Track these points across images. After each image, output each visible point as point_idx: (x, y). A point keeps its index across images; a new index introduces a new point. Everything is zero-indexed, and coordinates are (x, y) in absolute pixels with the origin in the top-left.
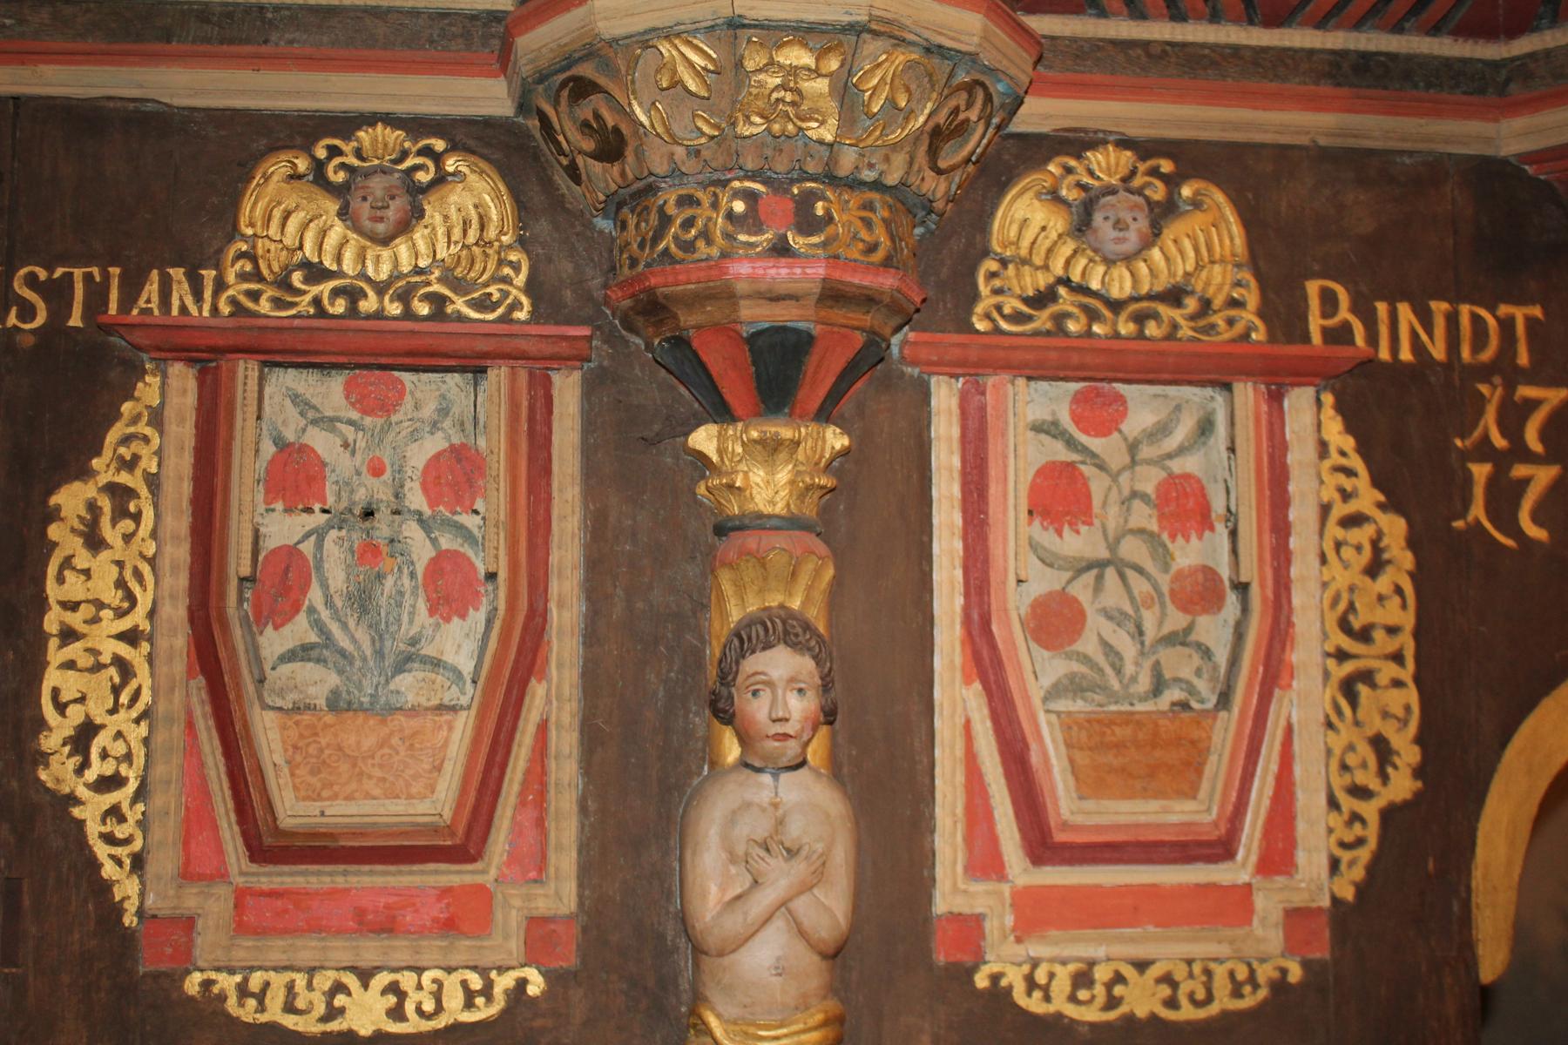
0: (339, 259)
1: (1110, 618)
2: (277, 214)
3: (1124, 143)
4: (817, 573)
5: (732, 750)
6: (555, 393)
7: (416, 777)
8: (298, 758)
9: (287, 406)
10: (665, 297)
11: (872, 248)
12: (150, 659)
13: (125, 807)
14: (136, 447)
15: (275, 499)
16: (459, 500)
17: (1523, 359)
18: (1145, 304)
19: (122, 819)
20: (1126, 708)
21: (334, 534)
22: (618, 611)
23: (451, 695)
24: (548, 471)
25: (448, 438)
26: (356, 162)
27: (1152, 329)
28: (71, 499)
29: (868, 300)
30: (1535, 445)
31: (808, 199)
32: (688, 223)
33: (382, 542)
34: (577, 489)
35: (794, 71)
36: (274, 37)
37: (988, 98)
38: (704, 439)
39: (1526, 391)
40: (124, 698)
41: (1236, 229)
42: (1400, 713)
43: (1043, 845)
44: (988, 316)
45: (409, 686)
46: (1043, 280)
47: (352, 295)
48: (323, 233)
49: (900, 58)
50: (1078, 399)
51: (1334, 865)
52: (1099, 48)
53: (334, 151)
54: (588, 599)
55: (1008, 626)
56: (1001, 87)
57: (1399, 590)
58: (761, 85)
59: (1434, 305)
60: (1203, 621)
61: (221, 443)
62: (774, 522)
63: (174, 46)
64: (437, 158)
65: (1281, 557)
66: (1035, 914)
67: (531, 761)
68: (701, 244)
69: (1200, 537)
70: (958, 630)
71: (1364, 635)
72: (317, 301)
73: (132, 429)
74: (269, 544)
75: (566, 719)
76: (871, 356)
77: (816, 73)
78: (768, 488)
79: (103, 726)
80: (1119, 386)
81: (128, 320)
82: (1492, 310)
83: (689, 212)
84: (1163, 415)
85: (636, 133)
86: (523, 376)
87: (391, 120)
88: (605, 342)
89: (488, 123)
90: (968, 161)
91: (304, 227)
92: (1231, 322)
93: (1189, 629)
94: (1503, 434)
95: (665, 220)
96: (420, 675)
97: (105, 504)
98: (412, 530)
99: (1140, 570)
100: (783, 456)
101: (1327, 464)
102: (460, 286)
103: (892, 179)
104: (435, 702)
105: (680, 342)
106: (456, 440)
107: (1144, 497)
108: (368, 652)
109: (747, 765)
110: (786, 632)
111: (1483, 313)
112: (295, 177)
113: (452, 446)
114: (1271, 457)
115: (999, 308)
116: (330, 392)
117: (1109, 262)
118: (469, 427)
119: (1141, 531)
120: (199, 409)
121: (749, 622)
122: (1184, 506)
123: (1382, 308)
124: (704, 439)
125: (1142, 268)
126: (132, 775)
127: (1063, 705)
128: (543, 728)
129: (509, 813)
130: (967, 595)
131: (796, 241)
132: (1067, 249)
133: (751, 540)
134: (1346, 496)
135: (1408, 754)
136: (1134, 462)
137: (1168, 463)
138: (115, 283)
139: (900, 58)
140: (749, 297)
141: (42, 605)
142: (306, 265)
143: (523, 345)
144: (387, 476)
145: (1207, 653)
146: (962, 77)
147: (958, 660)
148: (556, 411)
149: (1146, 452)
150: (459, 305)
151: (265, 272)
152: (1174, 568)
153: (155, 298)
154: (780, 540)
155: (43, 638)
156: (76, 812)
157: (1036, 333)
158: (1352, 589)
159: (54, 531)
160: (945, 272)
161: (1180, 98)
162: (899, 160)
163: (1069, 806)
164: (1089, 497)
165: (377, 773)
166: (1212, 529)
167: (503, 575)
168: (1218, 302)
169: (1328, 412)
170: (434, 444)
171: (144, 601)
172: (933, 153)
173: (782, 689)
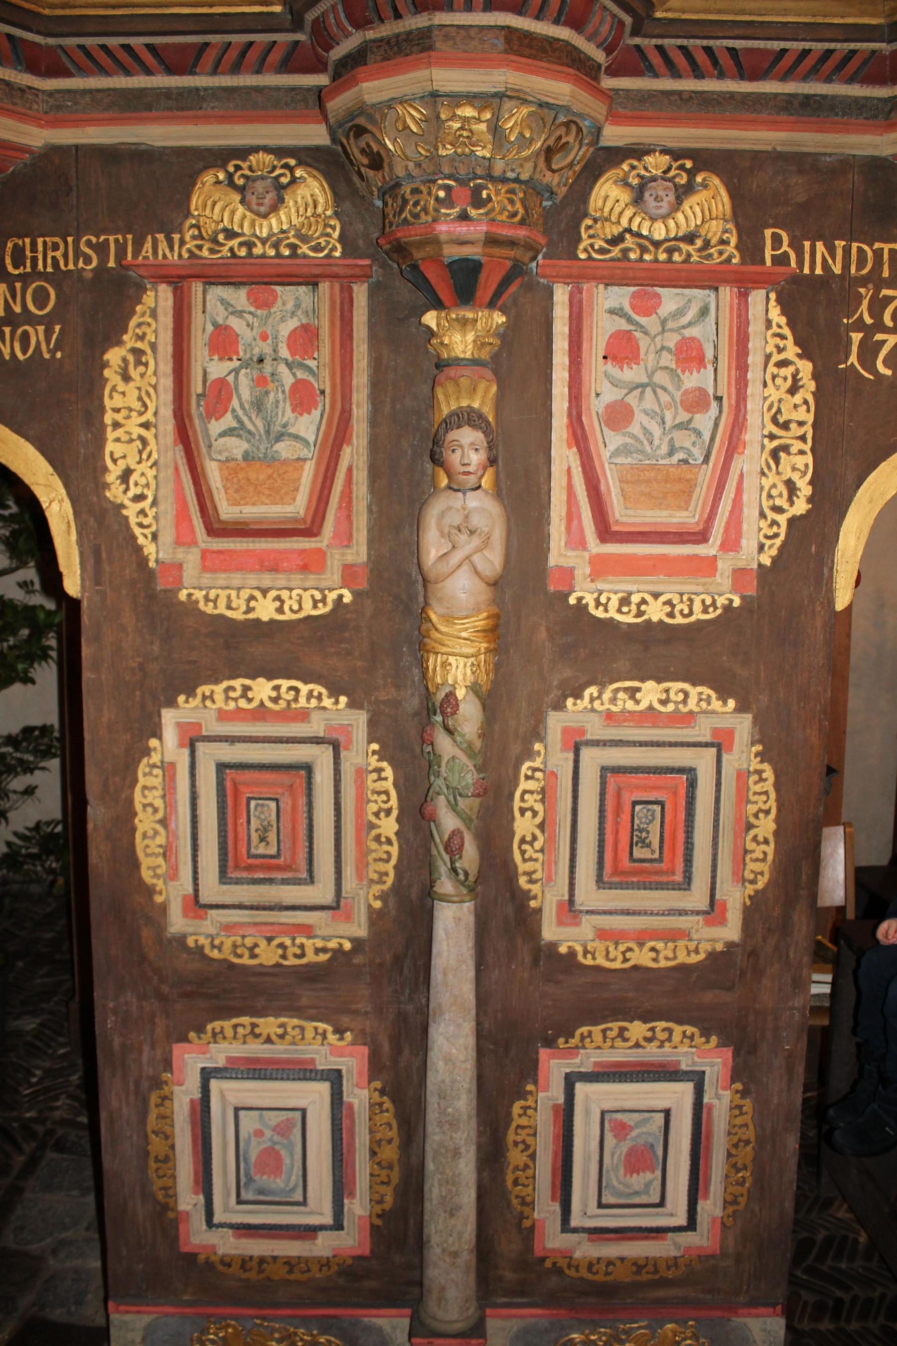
0: (242, 227)
1: (648, 415)
2: (209, 203)
3: (665, 152)
4: (487, 390)
5: (444, 482)
6: (354, 295)
7: (287, 493)
8: (228, 485)
10: (406, 243)
11: (514, 215)
12: (156, 436)
13: (147, 510)
14: (145, 328)
15: (213, 354)
16: (305, 352)
17: (886, 274)
18: (672, 243)
19: (146, 516)
20: (654, 462)
21: (243, 371)
22: (388, 409)
23: (304, 453)
24: (351, 337)
25: (300, 320)
26: (249, 173)
27: (676, 257)
28: (114, 356)
29: (512, 243)
30: (889, 323)
31: (478, 189)
32: (416, 204)
33: (268, 376)
34: (366, 346)
35: (466, 120)
36: (205, 106)
37: (580, 130)
39: (885, 292)
40: (144, 456)
41: (726, 199)
42: (802, 468)
43: (605, 533)
44: (585, 250)
45: (284, 449)
46: (616, 230)
47: (249, 245)
48: (233, 213)
49: (525, 111)
50: (634, 296)
51: (761, 548)
52: (654, 96)
53: (238, 168)
54: (372, 403)
55: (590, 417)
56: (587, 123)
57: (806, 402)
58: (450, 127)
59: (837, 243)
60: (698, 416)
61: (185, 325)
62: (464, 362)
63: (154, 113)
64: (291, 169)
65: (742, 383)
66: (601, 568)
67: (344, 486)
68: (422, 214)
69: (698, 372)
70: (565, 420)
71: (785, 426)
72: (231, 250)
73: (142, 320)
74: (212, 377)
75: (361, 465)
76: (517, 271)
77: (479, 120)
78: (461, 343)
79: (134, 470)
80: (657, 289)
81: (137, 262)
82: (871, 246)
83: (416, 197)
84: (681, 305)
85: (388, 155)
86: (337, 286)
87: (267, 150)
88: (381, 267)
89: (318, 149)
90: (571, 165)
91: (223, 209)
92: (721, 253)
93: (690, 421)
94: (871, 317)
95: (405, 202)
96: (288, 443)
97: (131, 358)
98: (283, 369)
99: (664, 389)
100: (469, 327)
101: (770, 332)
102: (304, 239)
103: (525, 177)
104: (296, 457)
105: (415, 267)
106: (304, 321)
107: (669, 350)
108: (262, 432)
109: (450, 488)
110: (469, 419)
111: (865, 247)
112: (218, 182)
113: (302, 325)
114: (739, 328)
115: (592, 246)
116: (240, 297)
117: (653, 219)
118: (311, 314)
119: (666, 368)
120: (174, 308)
121: (451, 415)
122: (690, 355)
123: (807, 244)
124: (430, 319)
125: (671, 224)
126: (150, 494)
127: (619, 460)
128: (350, 469)
129: (333, 512)
130: (570, 402)
131: (473, 212)
132: (629, 213)
133: (452, 372)
134: (780, 350)
135: (805, 490)
136: (663, 331)
137: (683, 331)
138: (130, 243)
139: (525, 111)
140: (447, 243)
141: (102, 410)
142: (225, 230)
143: (336, 269)
144: (269, 341)
145: (699, 434)
146: (562, 119)
147: (565, 436)
148: (355, 305)
149: (670, 325)
150: (304, 249)
151: (205, 234)
152: (683, 389)
153: (150, 250)
154: (467, 371)
155: (103, 427)
156: (125, 512)
157: (612, 260)
158: (780, 401)
160: (563, 226)
161: (697, 126)
162: (529, 166)
163: (622, 514)
164: (638, 349)
165: (267, 492)
166: (705, 367)
167: (328, 392)
168: (714, 241)
169: (772, 303)
170: (293, 324)
171: (152, 407)
172: (548, 161)
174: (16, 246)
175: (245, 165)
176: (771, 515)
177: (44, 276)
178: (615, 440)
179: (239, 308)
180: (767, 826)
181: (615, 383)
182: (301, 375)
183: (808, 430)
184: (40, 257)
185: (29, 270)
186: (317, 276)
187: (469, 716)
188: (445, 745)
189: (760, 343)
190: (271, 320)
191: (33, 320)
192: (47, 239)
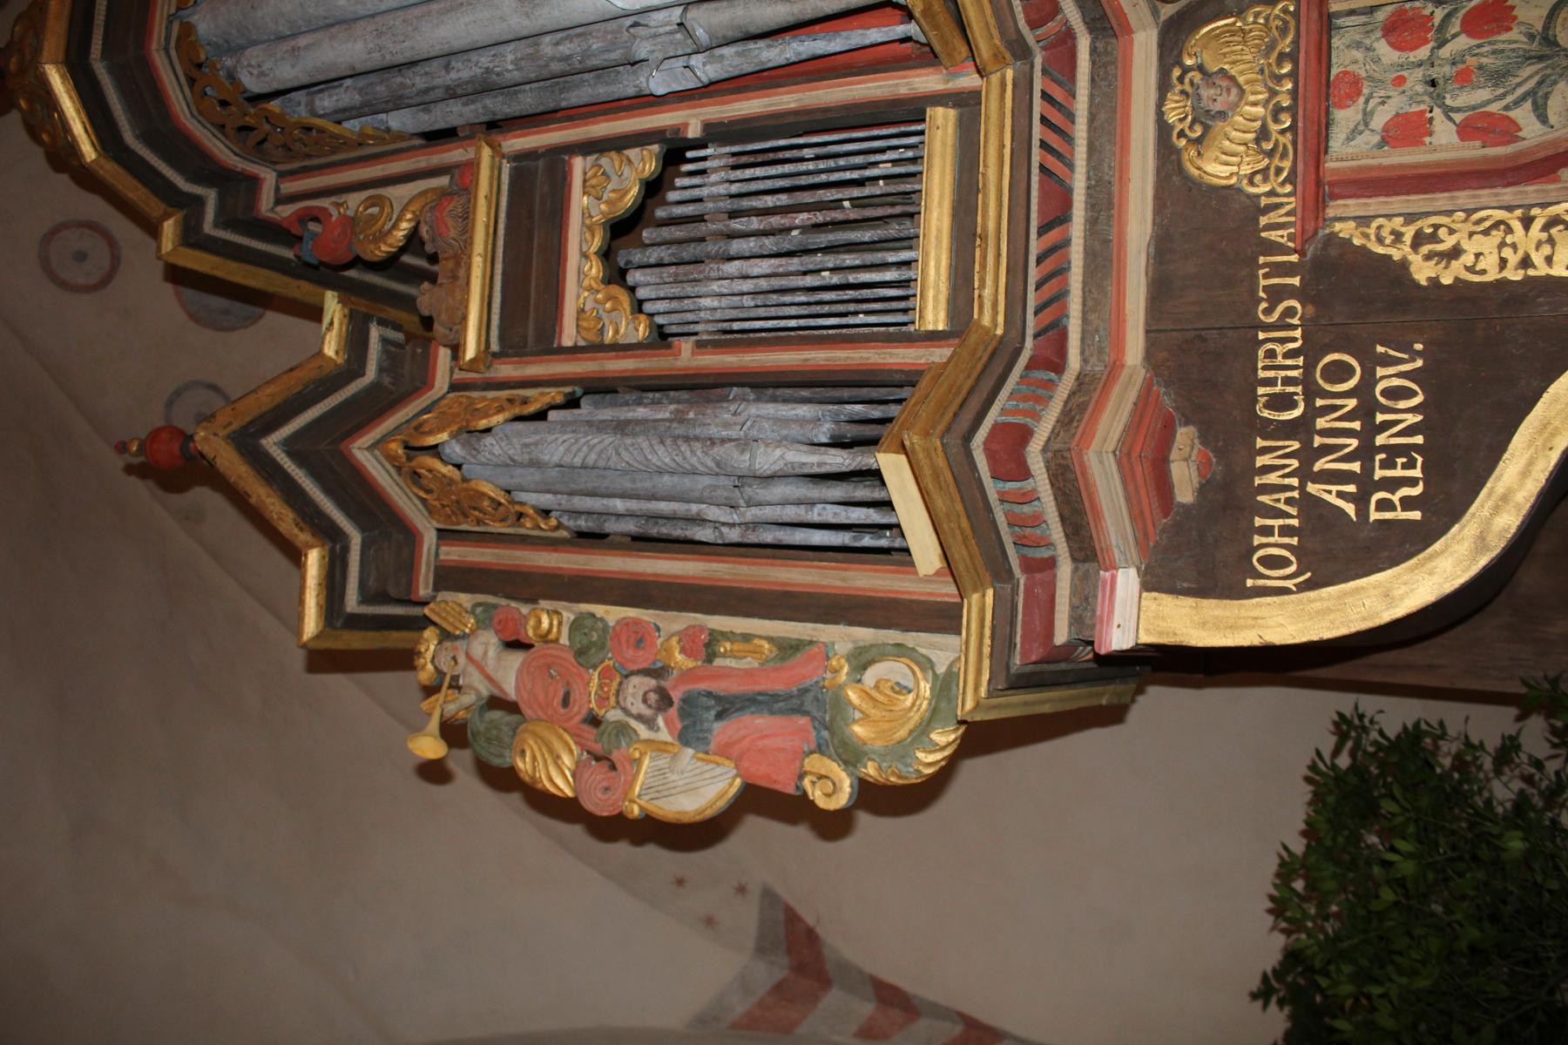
12: (1544, 206)
14: (1385, 233)
21: (1448, 102)
25: (1377, 39)
28: (1422, 271)
73: (1373, 237)
97: (1425, 249)
98: (1445, 52)
102: (1271, 47)
106: (1379, 34)
116: (1345, 117)
118: (1369, 28)
141: (1502, 284)
142: (1257, 141)
144: (1405, 73)
150: (1285, 45)
153: (1280, 233)
155: (1528, 280)
170: (1383, 49)
171: (1500, 214)
174: (1267, 406)
175: (1179, 127)
177: (1309, 368)
179: (1360, 117)
182: (1455, 26)
184: (1283, 373)
185: (1299, 389)
186: (1321, 15)
190: (1376, 75)
191: (1369, 380)
192: (1260, 365)
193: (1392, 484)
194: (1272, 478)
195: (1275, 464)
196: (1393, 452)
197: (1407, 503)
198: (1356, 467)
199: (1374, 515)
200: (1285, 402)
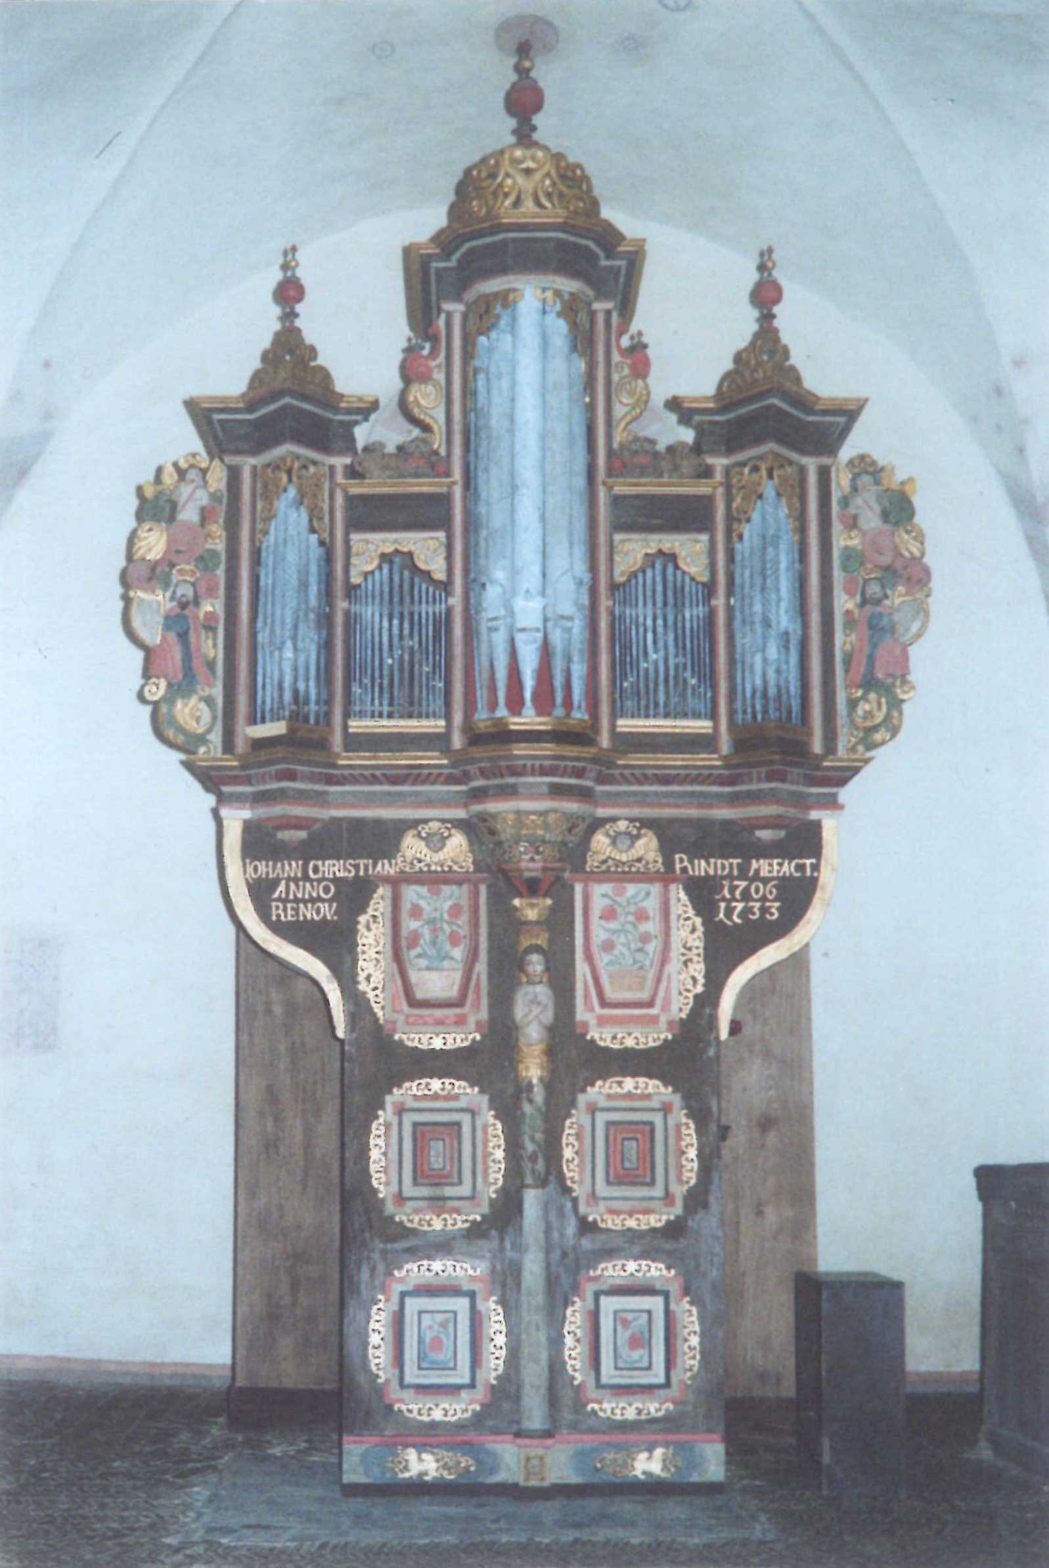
3: (626, 819)
9: (412, 894)
28: (363, 919)
29: (553, 869)
38: (517, 902)
39: (736, 883)
43: (604, 1003)
47: (429, 865)
51: (681, 1010)
66: (602, 1021)
71: (690, 949)
78: (532, 914)
98: (446, 926)
102: (456, 863)
116: (423, 890)
124: (517, 902)
126: (380, 986)
127: (611, 968)
128: (478, 975)
132: (609, 849)
135: (701, 980)
150: (455, 868)
155: (357, 954)
159: (359, 927)
170: (449, 903)
173: (536, 963)
176: (685, 994)
177: (328, 879)
178: (606, 958)
180: (692, 1153)
181: (607, 930)
183: (701, 951)
187: (539, 1095)
188: (527, 1108)
189: (676, 910)
191: (323, 901)
193: (285, 910)
194: (287, 868)
195: (293, 868)
196: (296, 910)
197: (278, 916)
198: (291, 897)
199: (274, 904)
200: (316, 870)
